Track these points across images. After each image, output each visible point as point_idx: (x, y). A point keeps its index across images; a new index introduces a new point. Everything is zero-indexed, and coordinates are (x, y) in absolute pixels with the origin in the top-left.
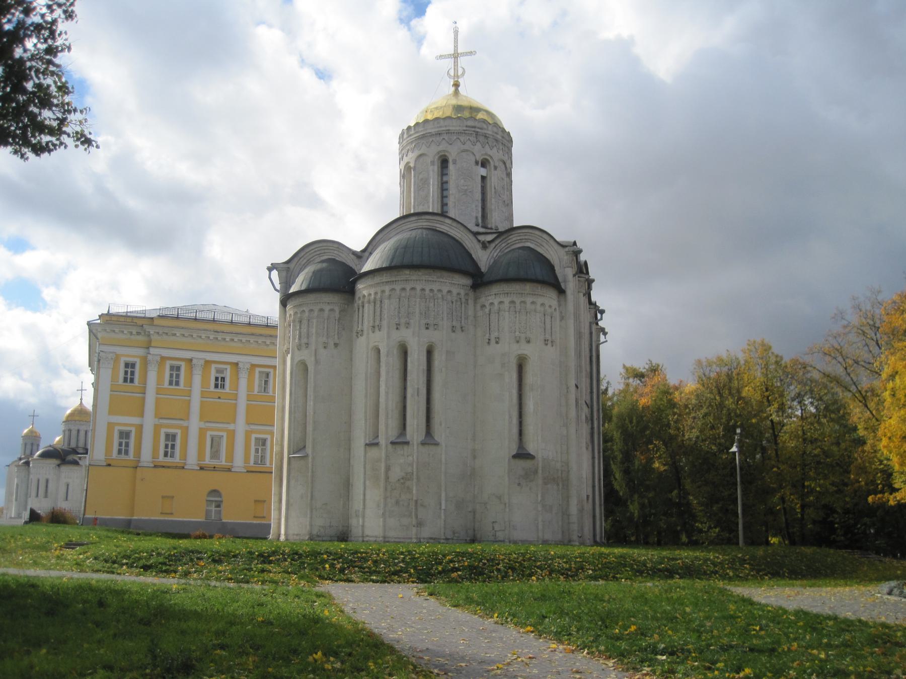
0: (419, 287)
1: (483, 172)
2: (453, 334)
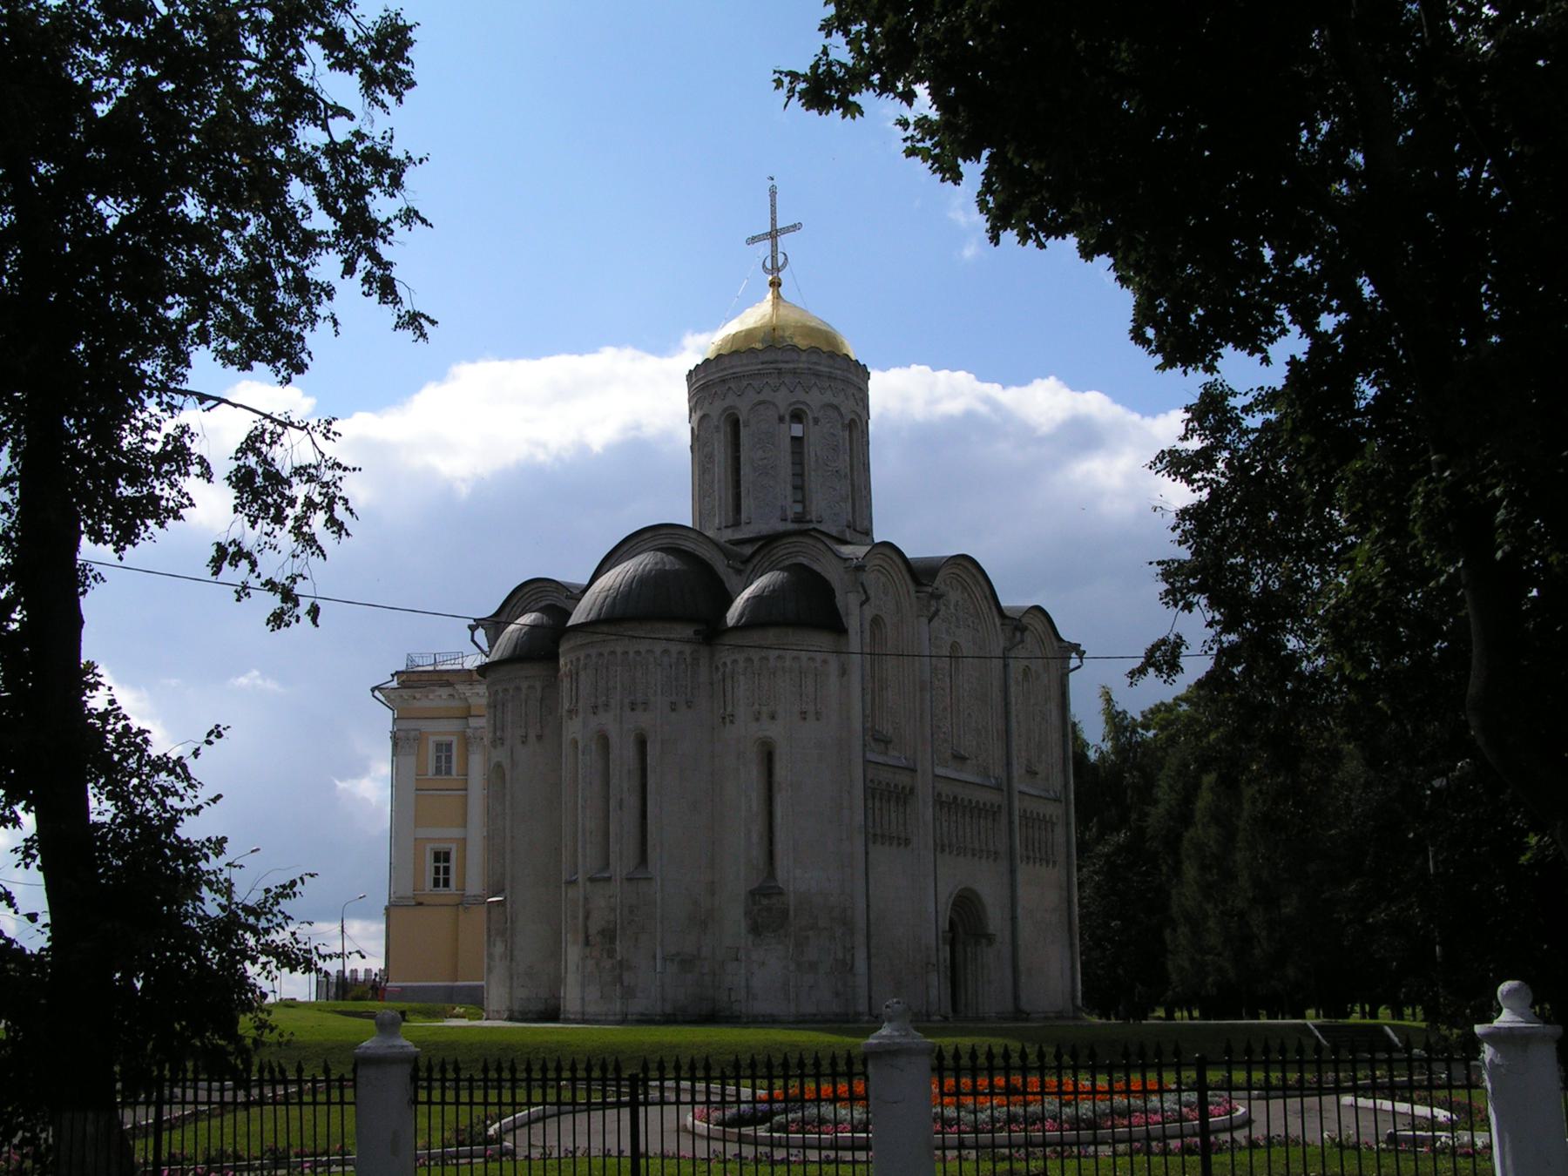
0: (619, 650)
1: (797, 430)
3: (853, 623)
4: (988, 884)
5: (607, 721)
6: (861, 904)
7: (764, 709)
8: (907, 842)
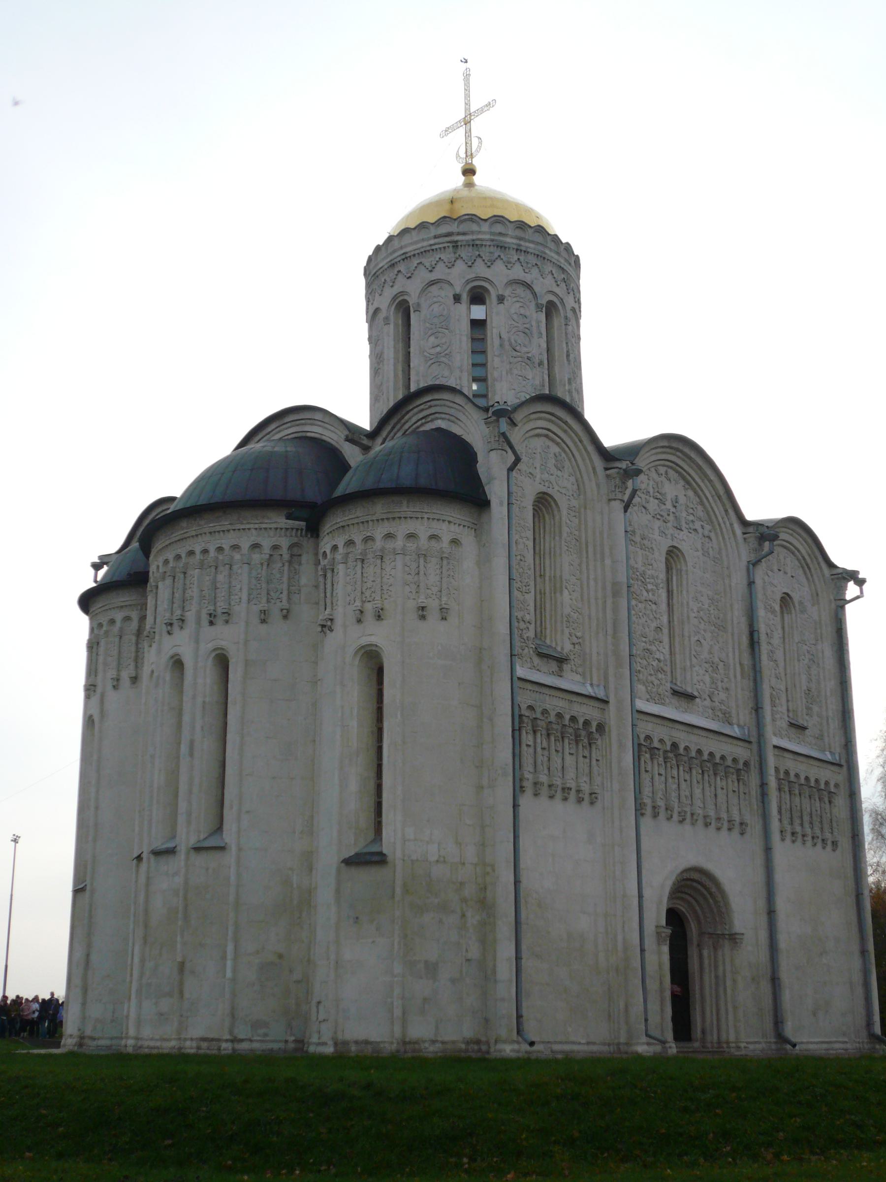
0: (198, 549)
1: (478, 312)
2: (265, 626)
3: (496, 491)
4: (732, 867)
6: (507, 877)
7: (369, 607)
8: (593, 798)
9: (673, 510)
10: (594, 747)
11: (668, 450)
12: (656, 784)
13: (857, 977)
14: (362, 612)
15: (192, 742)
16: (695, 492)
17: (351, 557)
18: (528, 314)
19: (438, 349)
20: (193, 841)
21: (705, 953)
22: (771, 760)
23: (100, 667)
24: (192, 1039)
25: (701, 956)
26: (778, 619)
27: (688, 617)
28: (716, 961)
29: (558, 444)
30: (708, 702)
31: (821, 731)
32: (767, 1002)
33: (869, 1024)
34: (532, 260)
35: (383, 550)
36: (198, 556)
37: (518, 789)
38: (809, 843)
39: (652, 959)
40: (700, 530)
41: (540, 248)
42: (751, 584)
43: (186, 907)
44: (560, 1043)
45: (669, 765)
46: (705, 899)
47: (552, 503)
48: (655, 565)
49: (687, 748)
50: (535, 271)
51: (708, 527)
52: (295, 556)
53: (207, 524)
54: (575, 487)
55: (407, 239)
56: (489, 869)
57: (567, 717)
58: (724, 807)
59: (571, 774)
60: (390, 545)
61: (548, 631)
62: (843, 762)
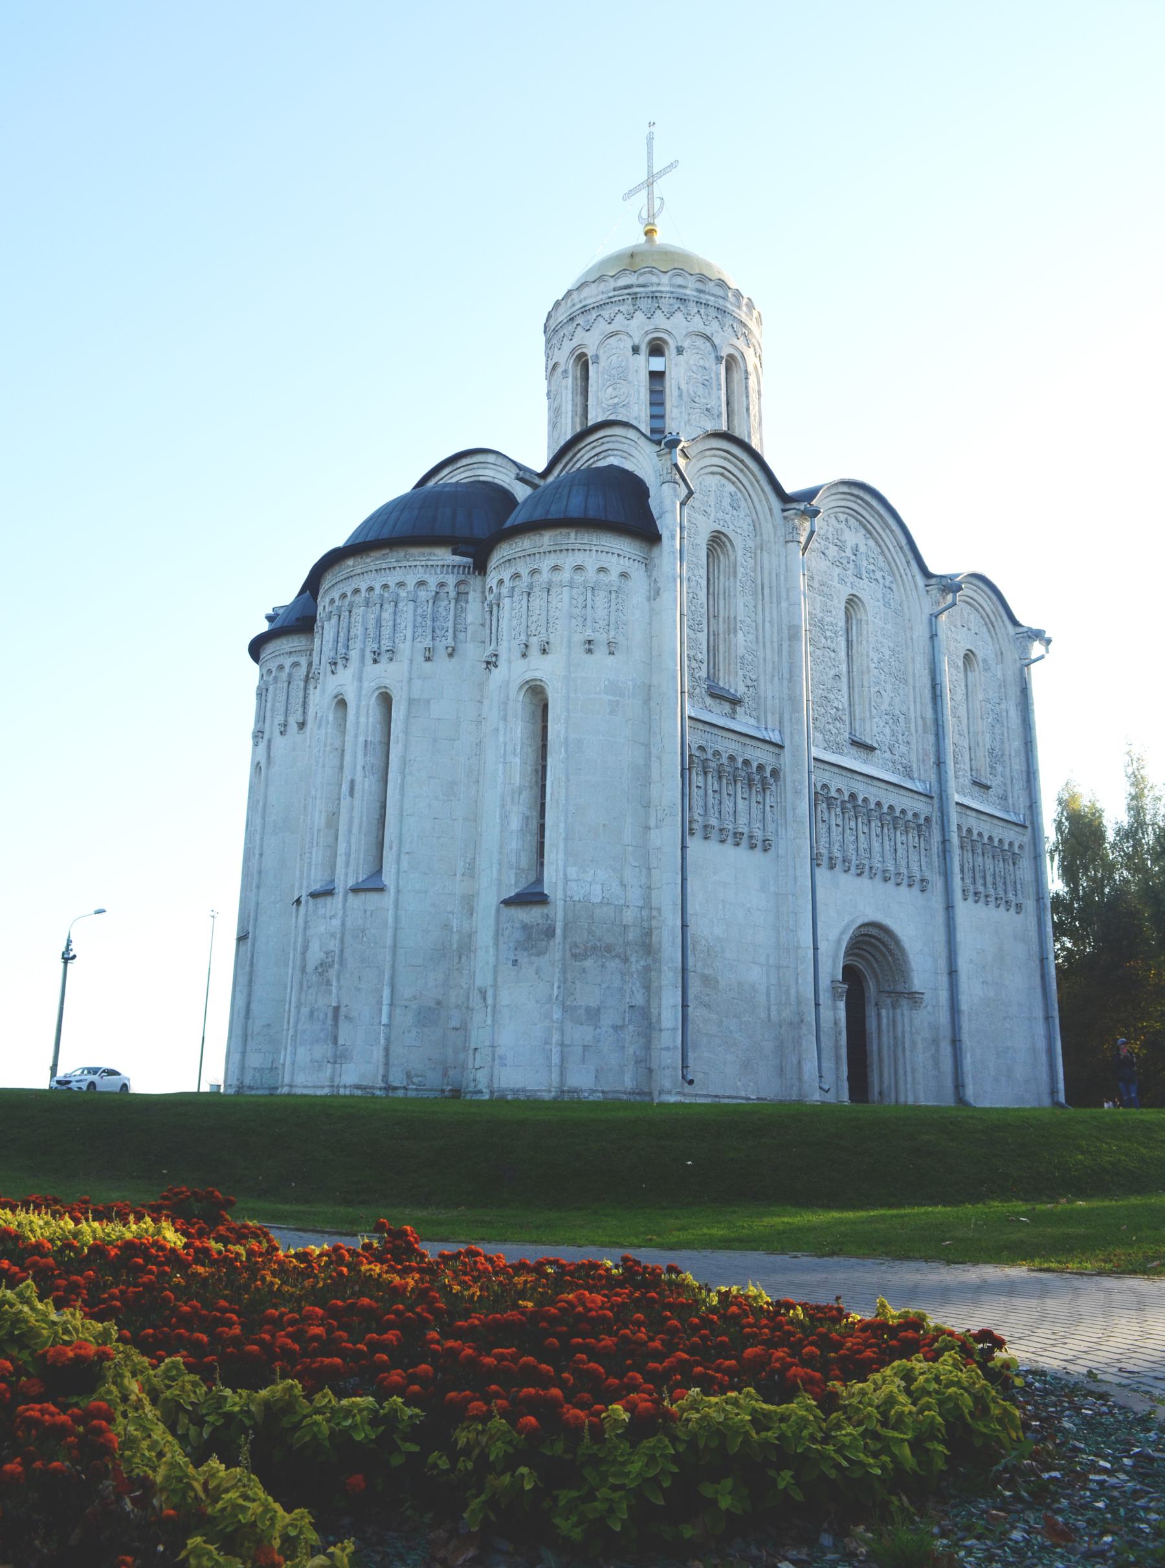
0: (364, 587)
1: (657, 364)
2: (429, 664)
5: (344, 680)
9: (853, 557)
10: (768, 792)
11: (848, 497)
12: (834, 834)
13: (1041, 1044)
14: (527, 646)
15: (352, 782)
16: (877, 542)
17: (517, 592)
18: (707, 366)
19: (616, 400)
20: (351, 883)
21: (884, 1012)
22: (954, 817)
23: (268, 714)
24: (345, 1087)
25: (879, 1015)
26: (962, 675)
27: (868, 667)
28: (894, 1021)
29: (733, 483)
30: (888, 755)
31: (1005, 791)
32: (947, 1064)
33: (1053, 1092)
34: (713, 313)
35: (550, 583)
36: (363, 593)
37: (688, 831)
38: (992, 905)
39: (826, 1014)
40: (881, 580)
41: (721, 301)
42: (933, 636)
43: (342, 951)
44: (729, 1097)
45: (846, 815)
46: (884, 955)
47: (728, 543)
48: (834, 613)
49: (865, 800)
50: (715, 324)
51: (891, 578)
52: (461, 596)
53: (371, 561)
54: (752, 527)
55: (586, 292)
56: (654, 913)
57: (740, 760)
58: (903, 863)
59: (742, 820)
60: (556, 577)
61: (721, 673)
62: (1028, 824)
